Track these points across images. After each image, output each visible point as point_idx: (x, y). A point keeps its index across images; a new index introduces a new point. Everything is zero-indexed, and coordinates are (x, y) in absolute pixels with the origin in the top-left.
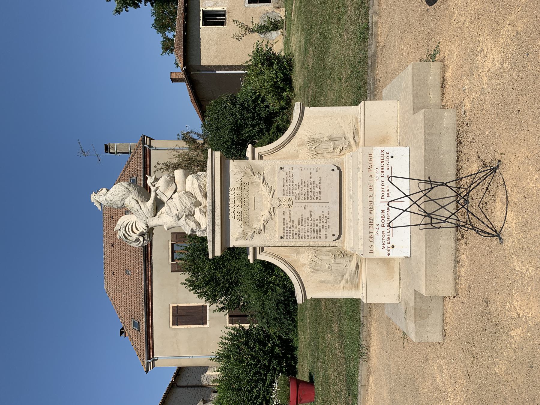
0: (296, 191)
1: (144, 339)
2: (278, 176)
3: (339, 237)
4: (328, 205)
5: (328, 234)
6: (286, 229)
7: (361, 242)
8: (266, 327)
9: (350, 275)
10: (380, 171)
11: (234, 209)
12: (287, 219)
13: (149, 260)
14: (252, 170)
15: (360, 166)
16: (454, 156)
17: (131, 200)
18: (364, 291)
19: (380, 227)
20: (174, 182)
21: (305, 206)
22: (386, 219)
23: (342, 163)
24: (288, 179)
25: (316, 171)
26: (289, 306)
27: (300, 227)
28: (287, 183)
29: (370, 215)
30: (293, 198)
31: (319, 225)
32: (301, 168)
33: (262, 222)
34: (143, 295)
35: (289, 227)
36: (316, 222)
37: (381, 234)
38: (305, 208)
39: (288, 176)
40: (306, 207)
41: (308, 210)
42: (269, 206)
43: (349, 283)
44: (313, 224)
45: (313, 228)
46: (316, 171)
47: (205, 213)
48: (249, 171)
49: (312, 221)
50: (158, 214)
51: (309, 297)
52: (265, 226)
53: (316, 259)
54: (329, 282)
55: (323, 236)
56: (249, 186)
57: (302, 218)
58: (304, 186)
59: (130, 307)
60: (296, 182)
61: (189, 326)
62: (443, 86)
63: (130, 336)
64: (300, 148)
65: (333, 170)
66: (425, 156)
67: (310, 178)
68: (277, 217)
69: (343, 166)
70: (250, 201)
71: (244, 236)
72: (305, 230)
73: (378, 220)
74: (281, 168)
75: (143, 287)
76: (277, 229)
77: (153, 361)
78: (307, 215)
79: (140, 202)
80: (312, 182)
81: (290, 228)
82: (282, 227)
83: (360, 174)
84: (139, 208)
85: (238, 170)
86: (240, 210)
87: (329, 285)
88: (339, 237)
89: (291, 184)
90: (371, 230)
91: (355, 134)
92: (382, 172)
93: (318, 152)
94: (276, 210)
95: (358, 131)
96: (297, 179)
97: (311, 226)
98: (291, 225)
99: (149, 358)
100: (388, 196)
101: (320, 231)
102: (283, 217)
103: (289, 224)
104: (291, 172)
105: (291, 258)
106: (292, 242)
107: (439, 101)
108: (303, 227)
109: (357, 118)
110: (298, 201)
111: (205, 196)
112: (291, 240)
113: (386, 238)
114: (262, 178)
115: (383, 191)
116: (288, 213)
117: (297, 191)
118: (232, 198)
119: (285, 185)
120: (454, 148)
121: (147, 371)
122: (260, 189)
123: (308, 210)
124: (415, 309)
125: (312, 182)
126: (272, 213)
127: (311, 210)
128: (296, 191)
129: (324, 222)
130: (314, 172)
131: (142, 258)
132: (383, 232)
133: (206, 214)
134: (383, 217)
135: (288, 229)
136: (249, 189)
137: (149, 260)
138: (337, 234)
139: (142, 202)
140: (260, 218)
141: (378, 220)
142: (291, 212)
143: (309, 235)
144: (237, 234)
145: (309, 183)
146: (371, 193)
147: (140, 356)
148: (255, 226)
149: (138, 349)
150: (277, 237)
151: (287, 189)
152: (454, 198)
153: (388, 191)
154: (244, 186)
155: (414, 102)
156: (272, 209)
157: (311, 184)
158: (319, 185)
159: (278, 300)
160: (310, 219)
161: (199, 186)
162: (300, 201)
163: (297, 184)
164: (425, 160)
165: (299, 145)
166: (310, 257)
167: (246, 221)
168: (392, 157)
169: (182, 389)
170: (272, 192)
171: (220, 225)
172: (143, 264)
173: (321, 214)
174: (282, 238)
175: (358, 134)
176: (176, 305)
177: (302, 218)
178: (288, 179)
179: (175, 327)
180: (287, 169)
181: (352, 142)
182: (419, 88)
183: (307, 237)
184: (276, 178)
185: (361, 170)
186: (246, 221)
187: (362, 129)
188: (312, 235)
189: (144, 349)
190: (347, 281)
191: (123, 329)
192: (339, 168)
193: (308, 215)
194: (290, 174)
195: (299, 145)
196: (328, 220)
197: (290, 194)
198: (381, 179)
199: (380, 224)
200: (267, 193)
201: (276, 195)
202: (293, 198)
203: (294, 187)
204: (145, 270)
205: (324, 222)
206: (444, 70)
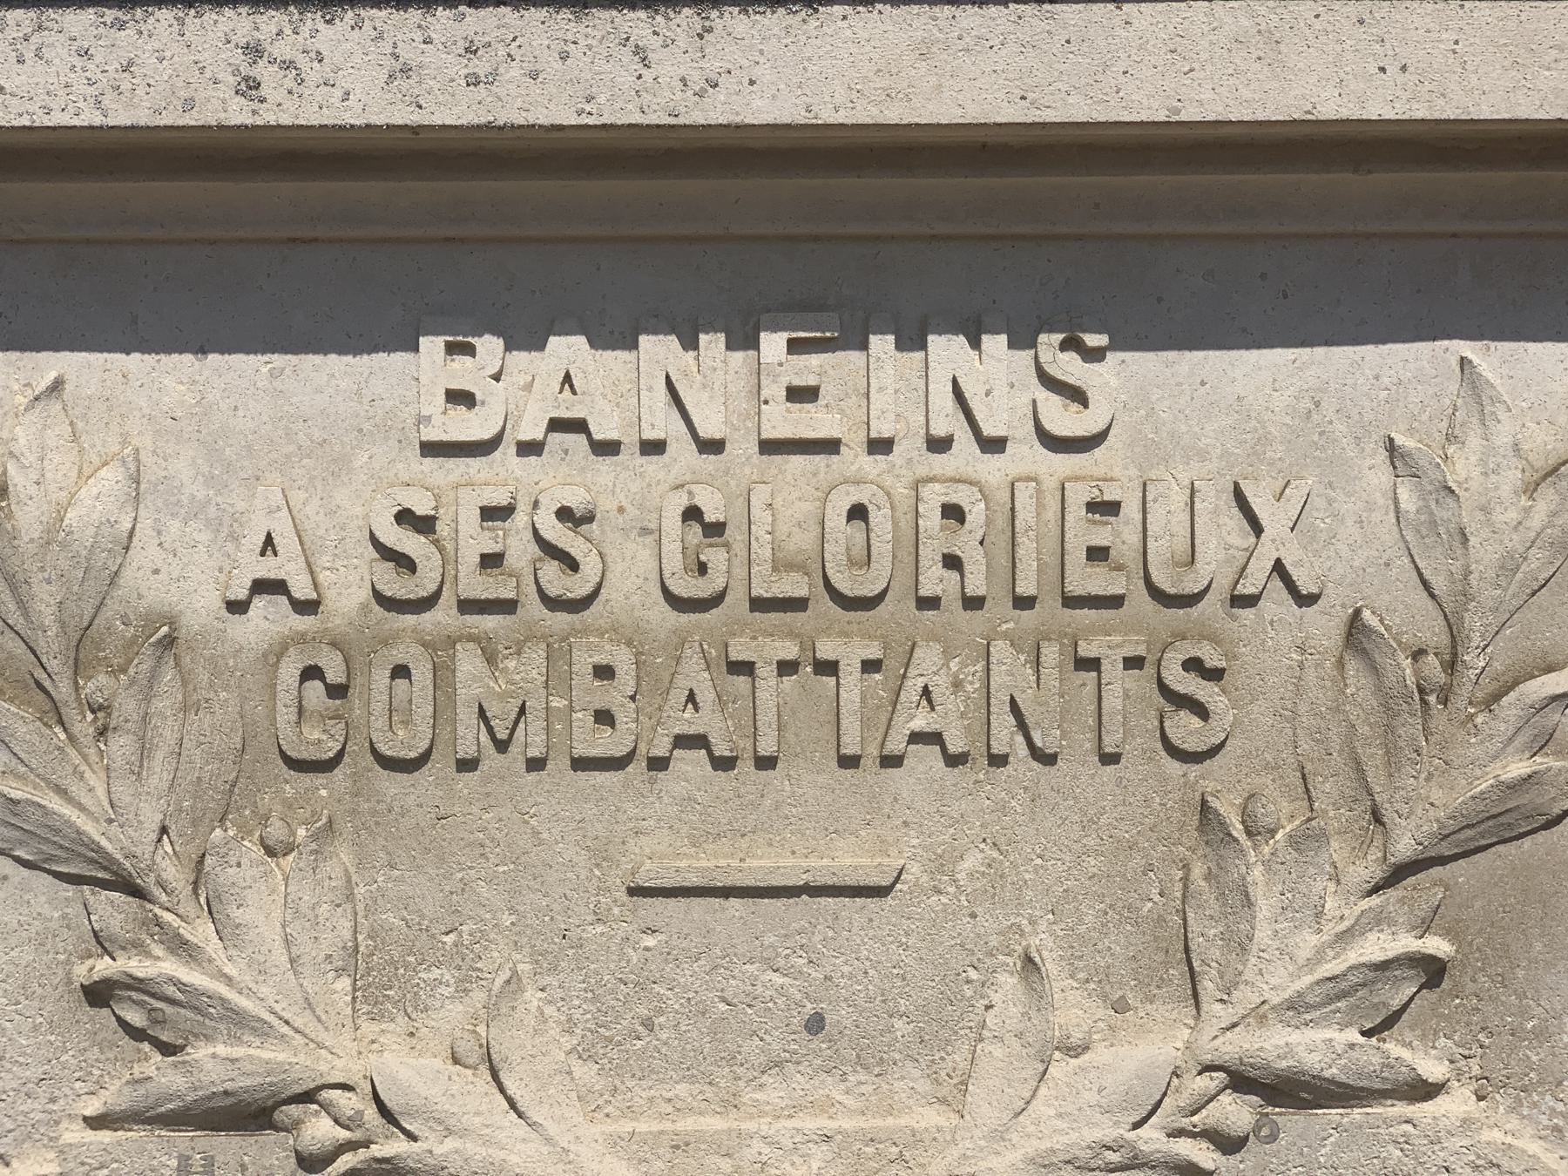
11: (641, 435)
14: (1504, 821)
33: (338, 1058)
56: (1146, 766)
70: (808, 781)
86: (629, 573)
114: (1319, 1046)
118: (885, 383)
122: (1074, 1010)
136: (1079, 768)
140: (451, 1015)
144: (96, 502)
148: (261, 895)
154: (1143, 643)
171: (288, 107)
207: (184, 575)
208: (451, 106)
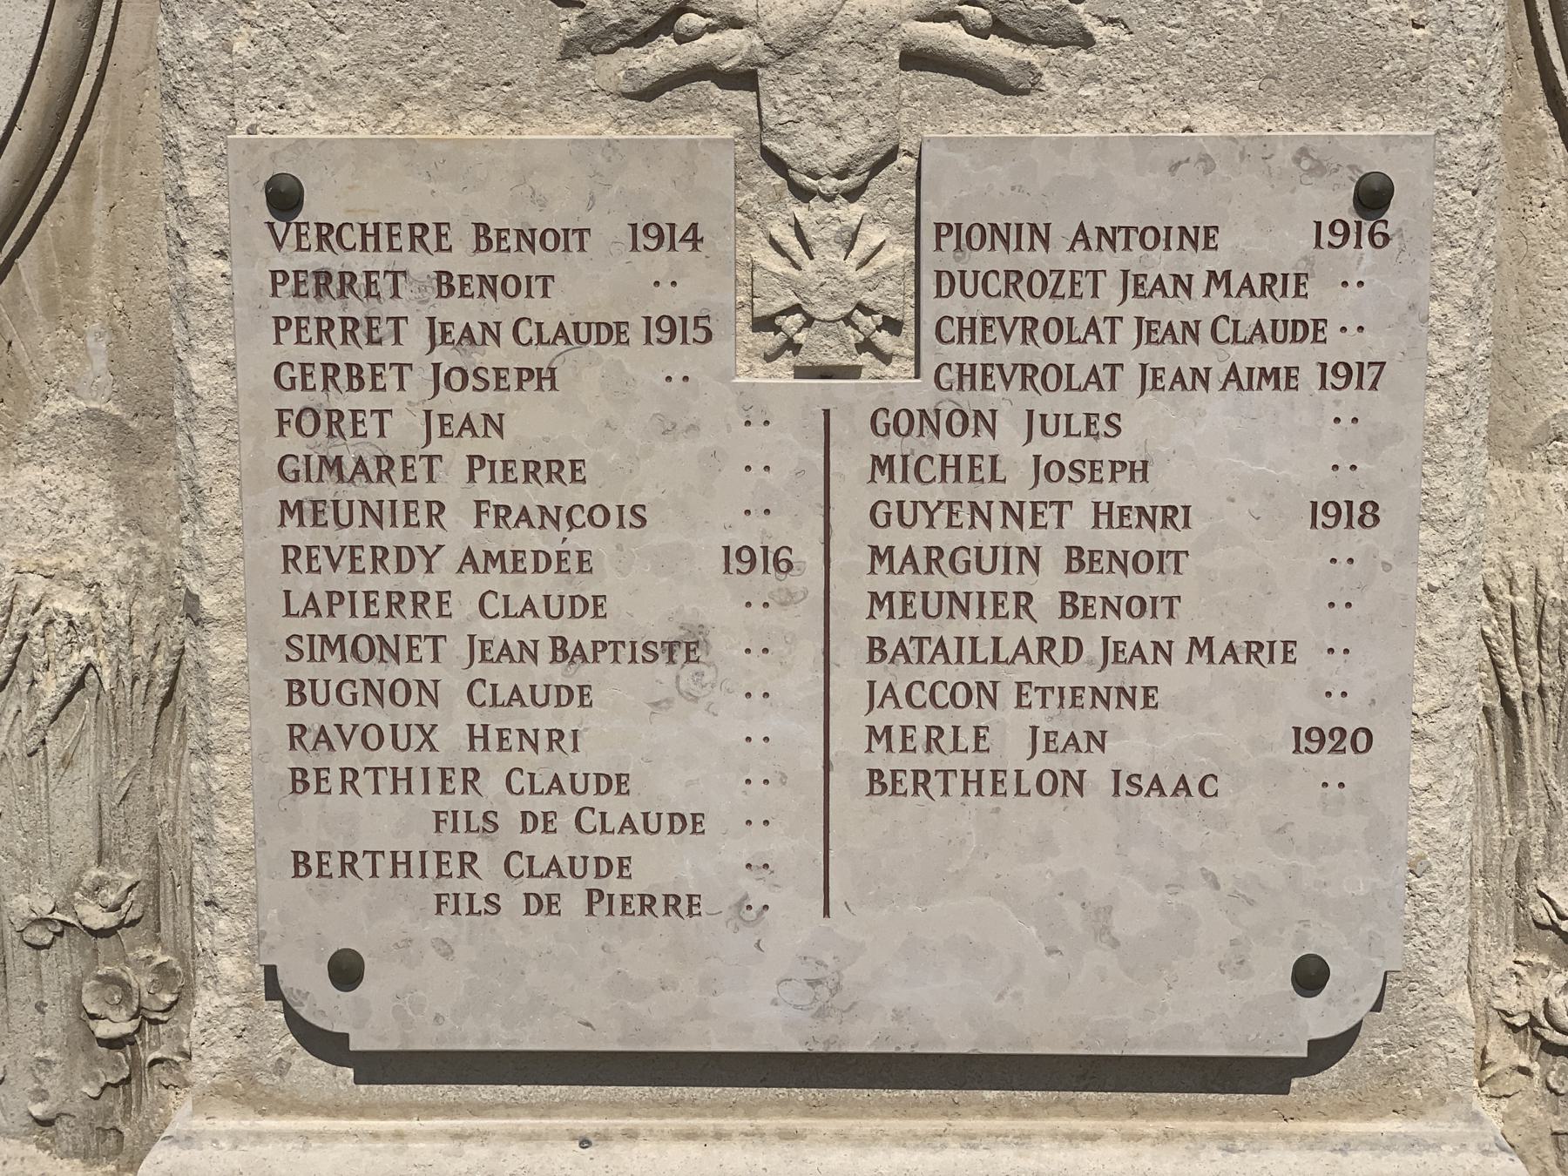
0: (1010, 429)
2: (1250, 152)
3: (326, 1045)
4: (792, 910)
5: (358, 890)
6: (423, 265)
12: (581, 288)
21: (780, 562)
23: (1395, 1092)
24: (1203, 307)
25: (1310, 739)
27: (451, 486)
28: (1133, 284)
30: (897, 383)
31: (494, 766)
32: (1369, 514)
35: (459, 312)
36: (541, 719)
38: (741, 559)
39: (1254, 310)
40: (763, 582)
44: (505, 676)
45: (452, 680)
46: (1310, 739)
49: (545, 671)
53: (52, 688)
55: (319, 822)
57: (599, 515)
58: (1077, 559)
60: (1147, 423)
65: (1310, 976)
67: (1202, 647)
68: (596, 127)
69: (1356, 1107)
72: (406, 558)
74: (1373, 198)
76: (423, 123)
78: (639, 599)
80: (1139, 675)
81: (438, 333)
82: (458, 208)
88: (326, 1045)
89: (1126, 349)
93: (1535, 733)
94: (714, 123)
96: (1213, 448)
97: (480, 650)
98: (489, 356)
101: (402, 781)
102: (609, 228)
103: (501, 310)
104: (1305, 356)
105: (44, 338)
106: (230, 368)
108: (459, 530)
110: (851, 465)
112: (263, 353)
116: (678, 303)
117: (1009, 441)
119: (1112, 262)
123: (720, 606)
125: (1139, 675)
126: (661, 56)
127: (725, 646)
128: (1010, 429)
129: (542, 846)
130: (1294, 697)
138: (368, 1019)
142: (681, 357)
143: (345, 624)
145: (1126, 629)
150: (307, 127)
151: (1048, 284)
156: (729, 46)
157: (1112, 651)
158: (1097, 767)
160: (581, 631)
162: (851, 465)
163: (1123, 449)
166: (72, 603)
170: (998, 50)
174: (284, 199)
177: (599, 515)
178: (1203, 307)
180: (1357, 295)
183: (304, 584)
184: (1215, 122)
188: (334, 668)
192: (1326, 1052)
193: (639, 599)
194: (1278, 342)
196: (573, 895)
197: (971, 329)
201: (960, 123)
202: (897, 383)
203: (1077, 404)
205: (542, 846)
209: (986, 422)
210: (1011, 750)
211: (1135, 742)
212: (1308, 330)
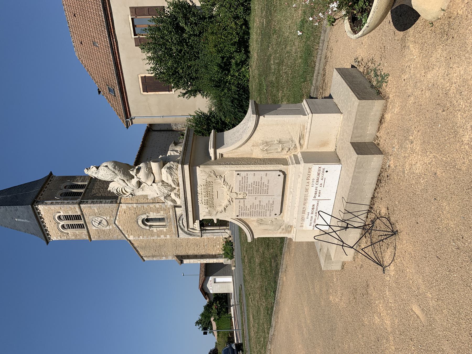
1: (121, 103)
7: (295, 220)
8: (223, 117)
9: (286, 226)
10: (315, 181)
13: (113, 34)
15: (301, 175)
16: (374, 186)
17: (119, 180)
18: (294, 235)
19: (310, 214)
20: (152, 173)
22: (315, 210)
24: (243, 181)
26: (242, 101)
29: (304, 206)
34: (113, 66)
37: (310, 218)
38: (256, 199)
39: (244, 179)
41: (258, 200)
42: (229, 197)
43: (284, 231)
47: (179, 195)
48: (212, 174)
50: (141, 186)
51: (256, 237)
52: (225, 209)
54: (270, 230)
59: (104, 76)
60: (249, 182)
61: (157, 93)
62: (381, 122)
63: (108, 99)
64: (255, 148)
65: (279, 175)
66: (351, 186)
68: (234, 203)
69: (288, 171)
71: (210, 213)
73: (309, 210)
75: (112, 60)
76: (234, 210)
77: (131, 120)
78: (257, 202)
79: (126, 181)
83: (300, 180)
84: (126, 185)
85: (203, 174)
87: (270, 231)
90: (303, 215)
91: (301, 138)
92: (317, 181)
95: (304, 135)
99: (127, 118)
100: (319, 196)
107: (375, 132)
109: (304, 126)
111: (178, 185)
113: (313, 220)
114: (223, 180)
115: (316, 194)
120: (375, 181)
121: (127, 127)
123: (258, 200)
124: (326, 255)
126: (231, 201)
131: (106, 33)
132: (312, 217)
133: (180, 196)
134: (313, 209)
135: (243, 211)
137: (113, 34)
139: (127, 180)
141: (309, 210)
146: (306, 193)
147: (120, 115)
149: (116, 110)
152: (366, 211)
153: (320, 193)
154: (208, 184)
155: (353, 133)
156: (231, 199)
159: (233, 97)
161: (173, 181)
164: (350, 189)
165: (253, 146)
167: (211, 204)
168: (327, 171)
169: (156, 132)
172: (108, 38)
173: (267, 202)
175: (303, 138)
176: (143, 75)
179: (146, 93)
181: (298, 145)
182: (360, 121)
185: (301, 177)
186: (211, 204)
187: (307, 135)
189: (122, 110)
190: (283, 229)
191: (99, 89)
195: (253, 146)
198: (315, 186)
199: (310, 212)
200: (227, 189)
201: (234, 190)
202: (247, 193)
204: (111, 44)
206: (385, 109)
207: (207, 210)
208: (191, 209)
209: (249, 190)
210: (266, 188)
211: (266, 183)
212: (245, 177)
